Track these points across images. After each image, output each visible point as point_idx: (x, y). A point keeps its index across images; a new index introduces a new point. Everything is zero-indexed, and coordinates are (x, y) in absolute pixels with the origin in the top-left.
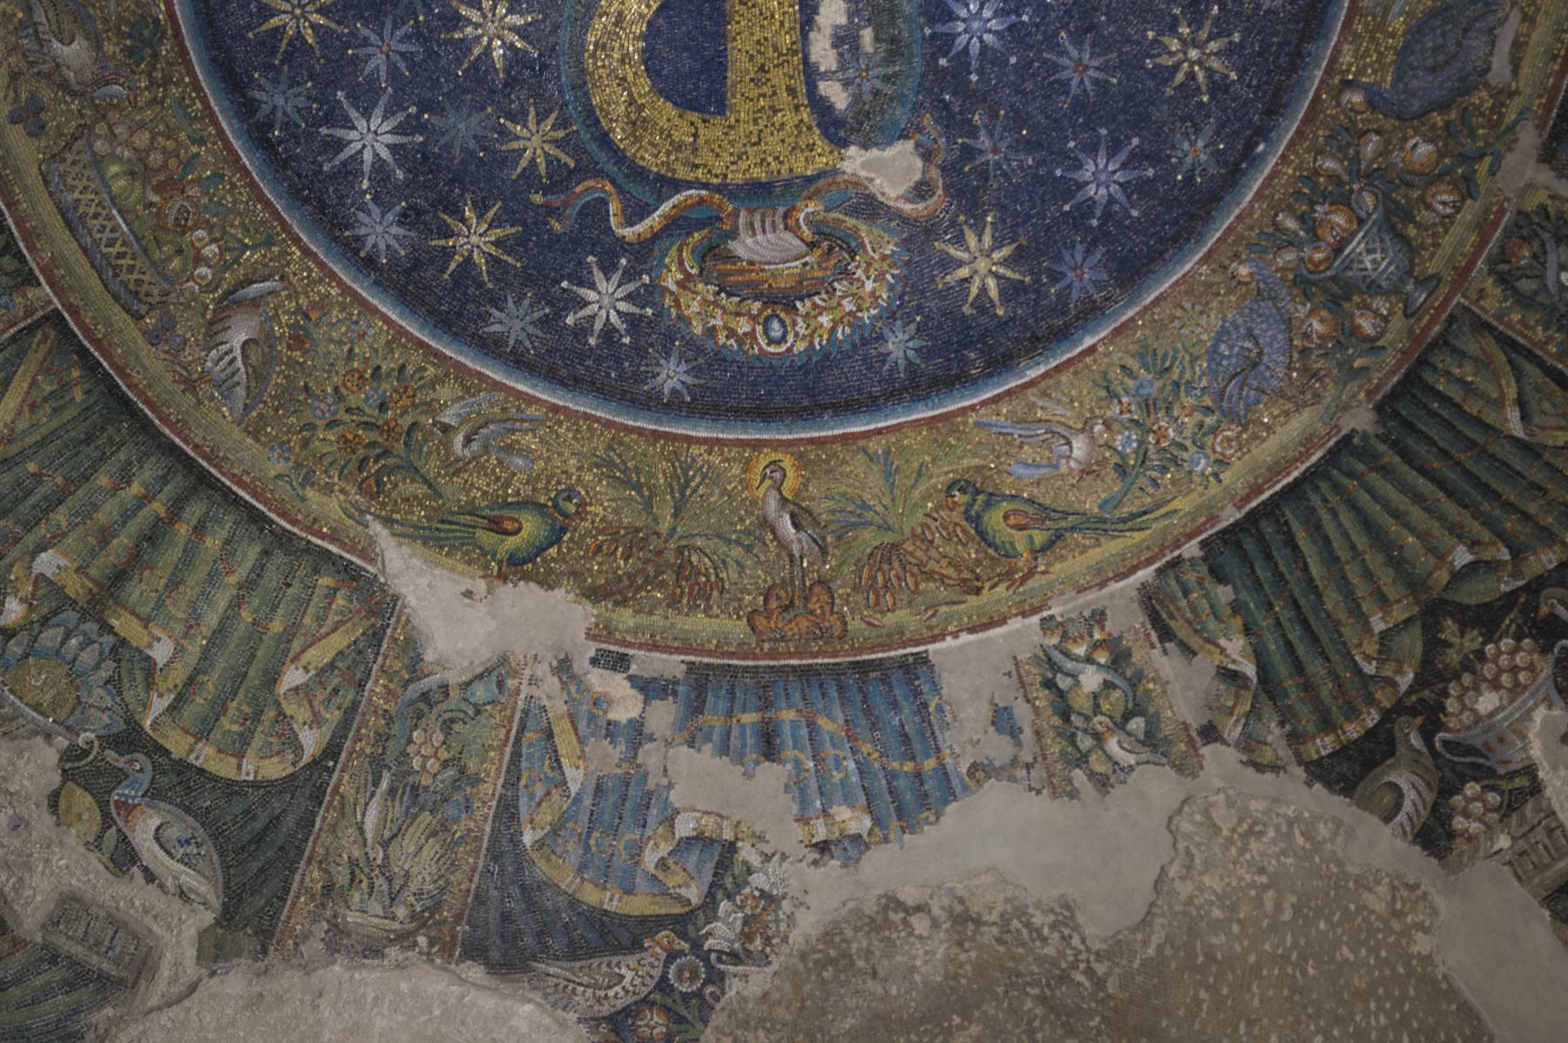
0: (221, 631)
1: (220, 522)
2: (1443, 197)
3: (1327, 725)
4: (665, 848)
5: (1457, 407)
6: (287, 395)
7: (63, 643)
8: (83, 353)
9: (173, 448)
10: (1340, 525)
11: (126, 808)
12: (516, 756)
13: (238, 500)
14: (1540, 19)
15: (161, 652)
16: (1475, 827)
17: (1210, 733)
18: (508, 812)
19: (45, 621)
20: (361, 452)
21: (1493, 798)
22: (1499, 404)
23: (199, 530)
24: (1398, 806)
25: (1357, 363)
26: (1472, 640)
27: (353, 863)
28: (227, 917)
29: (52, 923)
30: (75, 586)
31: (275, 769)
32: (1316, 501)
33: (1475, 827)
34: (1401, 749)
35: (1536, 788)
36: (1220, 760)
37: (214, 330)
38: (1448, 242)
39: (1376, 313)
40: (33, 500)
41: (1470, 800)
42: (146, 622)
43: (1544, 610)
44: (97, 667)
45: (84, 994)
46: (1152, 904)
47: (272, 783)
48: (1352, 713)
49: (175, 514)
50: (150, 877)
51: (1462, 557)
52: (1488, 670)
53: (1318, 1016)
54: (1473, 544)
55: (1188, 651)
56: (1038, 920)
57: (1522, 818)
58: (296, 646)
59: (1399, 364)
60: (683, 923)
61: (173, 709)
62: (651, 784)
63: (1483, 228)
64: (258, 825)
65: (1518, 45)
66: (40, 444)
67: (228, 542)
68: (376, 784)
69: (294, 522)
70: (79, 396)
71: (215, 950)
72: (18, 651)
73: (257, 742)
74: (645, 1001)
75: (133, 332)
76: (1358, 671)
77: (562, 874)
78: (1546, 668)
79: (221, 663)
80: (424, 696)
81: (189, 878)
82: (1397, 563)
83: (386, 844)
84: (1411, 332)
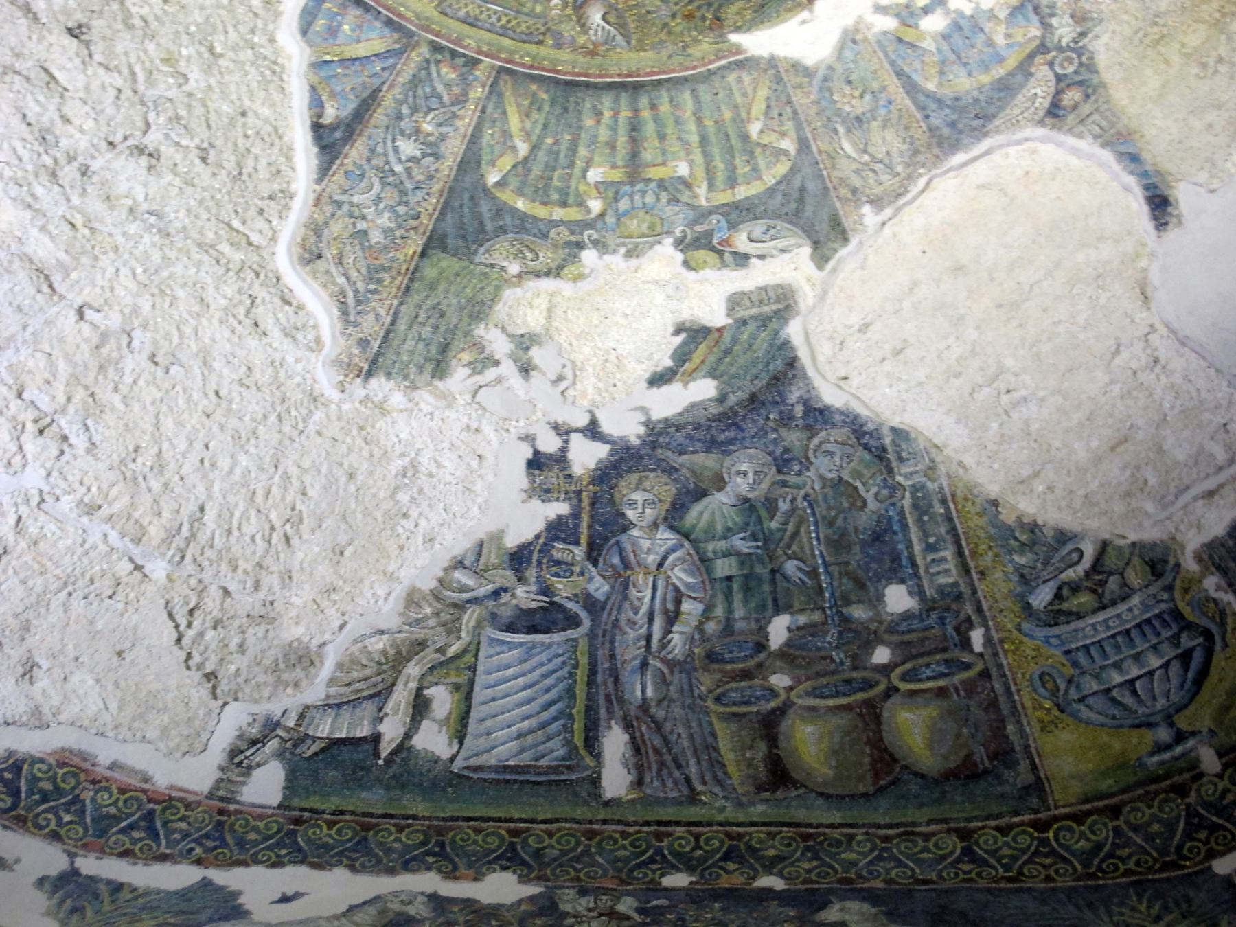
0: (704, 141)
1: (659, 97)
4: (1002, 29)
6: (643, 20)
7: (632, 201)
8: (533, 78)
9: (610, 86)
11: (726, 242)
12: (893, 63)
13: (659, 82)
15: (683, 170)
18: (911, 88)
19: (616, 200)
20: (698, 14)
23: (653, 107)
27: (857, 172)
28: (816, 245)
29: (731, 310)
30: (617, 175)
31: (782, 168)
37: (584, 27)
40: (562, 155)
42: (664, 164)
44: (658, 200)
45: (774, 325)
47: (785, 176)
49: (636, 111)
50: (761, 257)
58: (744, 115)
60: (1043, 48)
61: (711, 186)
62: (968, 12)
64: (796, 196)
66: (545, 126)
67: (671, 101)
68: (835, 131)
69: (694, 68)
70: (545, 96)
71: (821, 258)
72: (613, 220)
73: (762, 163)
74: (1058, 92)
75: (543, 51)
77: (963, 83)
79: (716, 151)
80: (825, 79)
81: (780, 243)
83: (865, 151)
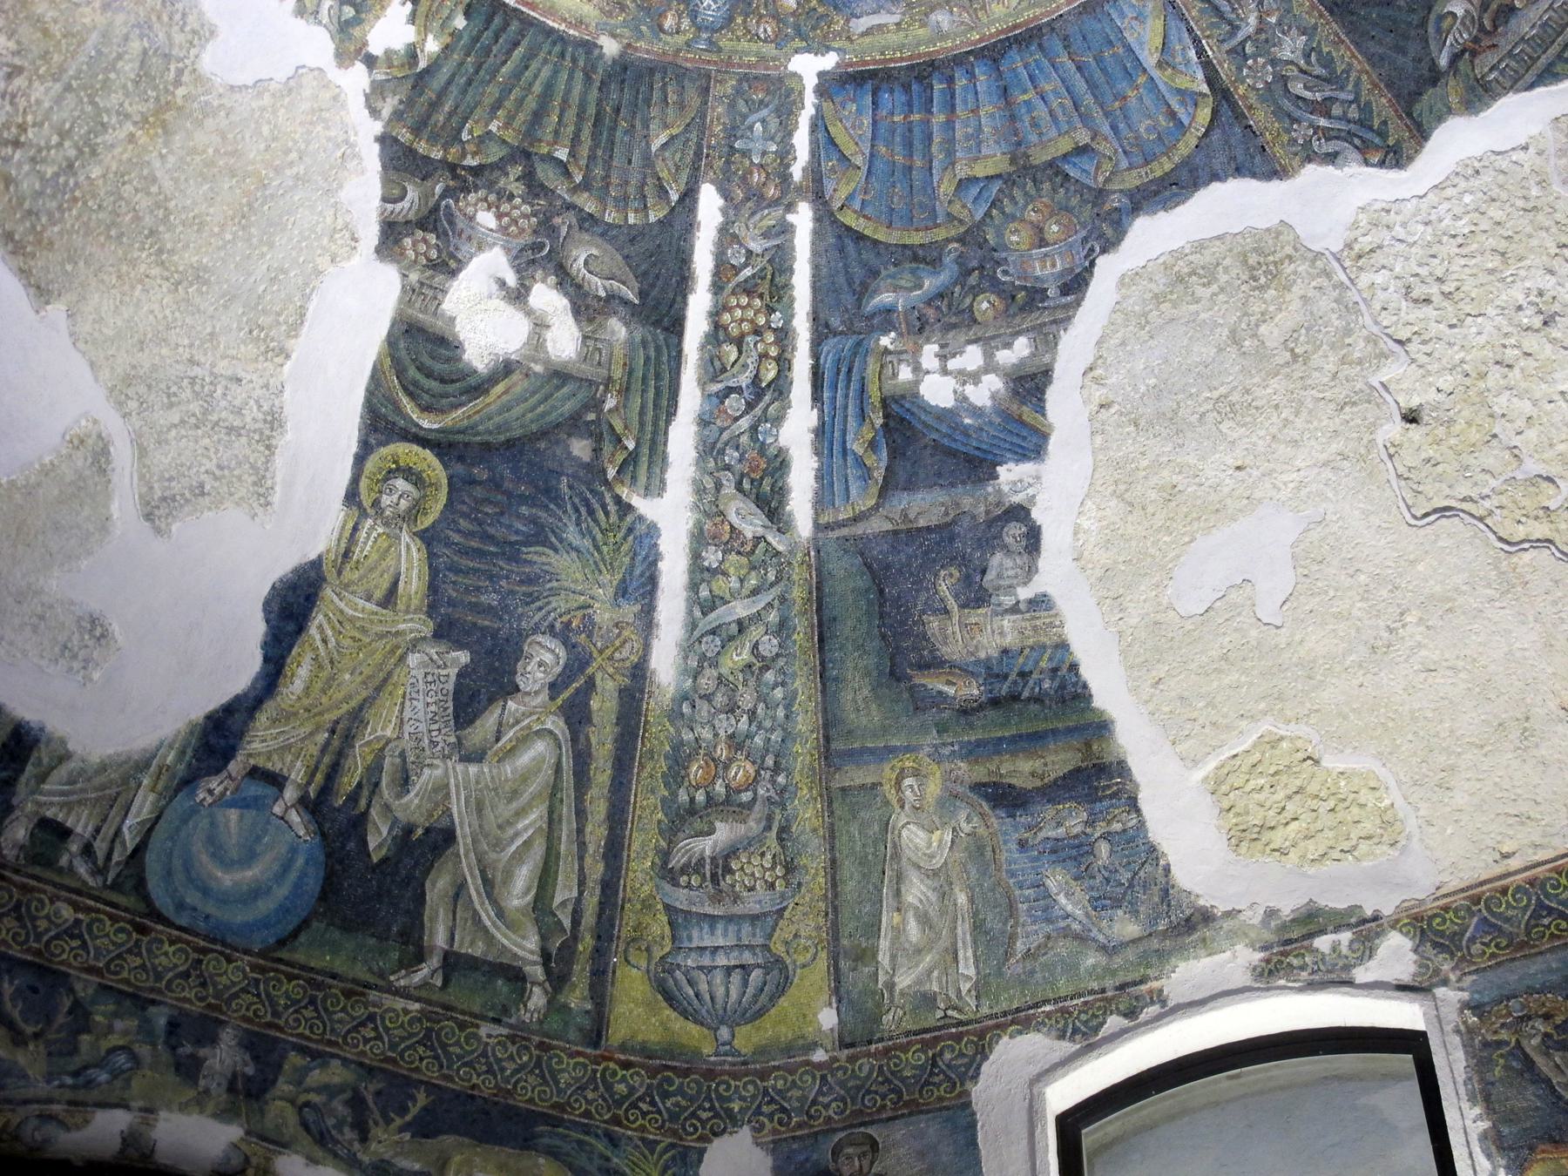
2: (769, 28)
3: (416, 131)
5: (648, 102)
10: (539, 70)
14: (902, 34)
16: (411, 254)
17: (370, 61)
21: (434, 254)
22: (666, 126)
24: (394, 201)
25: (644, 28)
26: (518, 188)
32: (546, 47)
33: (411, 254)
34: (429, 183)
35: (453, 273)
36: (356, 79)
38: (744, 44)
39: (679, 24)
41: (425, 241)
43: (557, 220)
46: (247, 87)
48: (433, 139)
51: (562, 154)
52: (505, 207)
53: (244, 228)
54: (572, 154)
55: (412, 19)
56: (190, 19)
57: (433, 277)
59: (657, 53)
63: (763, 59)
65: (880, 27)
76: (460, 131)
78: (528, 239)
82: (538, 116)
84: (679, 50)
